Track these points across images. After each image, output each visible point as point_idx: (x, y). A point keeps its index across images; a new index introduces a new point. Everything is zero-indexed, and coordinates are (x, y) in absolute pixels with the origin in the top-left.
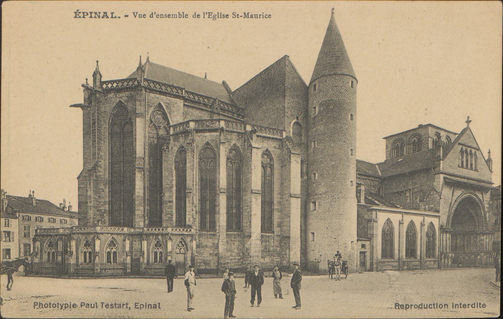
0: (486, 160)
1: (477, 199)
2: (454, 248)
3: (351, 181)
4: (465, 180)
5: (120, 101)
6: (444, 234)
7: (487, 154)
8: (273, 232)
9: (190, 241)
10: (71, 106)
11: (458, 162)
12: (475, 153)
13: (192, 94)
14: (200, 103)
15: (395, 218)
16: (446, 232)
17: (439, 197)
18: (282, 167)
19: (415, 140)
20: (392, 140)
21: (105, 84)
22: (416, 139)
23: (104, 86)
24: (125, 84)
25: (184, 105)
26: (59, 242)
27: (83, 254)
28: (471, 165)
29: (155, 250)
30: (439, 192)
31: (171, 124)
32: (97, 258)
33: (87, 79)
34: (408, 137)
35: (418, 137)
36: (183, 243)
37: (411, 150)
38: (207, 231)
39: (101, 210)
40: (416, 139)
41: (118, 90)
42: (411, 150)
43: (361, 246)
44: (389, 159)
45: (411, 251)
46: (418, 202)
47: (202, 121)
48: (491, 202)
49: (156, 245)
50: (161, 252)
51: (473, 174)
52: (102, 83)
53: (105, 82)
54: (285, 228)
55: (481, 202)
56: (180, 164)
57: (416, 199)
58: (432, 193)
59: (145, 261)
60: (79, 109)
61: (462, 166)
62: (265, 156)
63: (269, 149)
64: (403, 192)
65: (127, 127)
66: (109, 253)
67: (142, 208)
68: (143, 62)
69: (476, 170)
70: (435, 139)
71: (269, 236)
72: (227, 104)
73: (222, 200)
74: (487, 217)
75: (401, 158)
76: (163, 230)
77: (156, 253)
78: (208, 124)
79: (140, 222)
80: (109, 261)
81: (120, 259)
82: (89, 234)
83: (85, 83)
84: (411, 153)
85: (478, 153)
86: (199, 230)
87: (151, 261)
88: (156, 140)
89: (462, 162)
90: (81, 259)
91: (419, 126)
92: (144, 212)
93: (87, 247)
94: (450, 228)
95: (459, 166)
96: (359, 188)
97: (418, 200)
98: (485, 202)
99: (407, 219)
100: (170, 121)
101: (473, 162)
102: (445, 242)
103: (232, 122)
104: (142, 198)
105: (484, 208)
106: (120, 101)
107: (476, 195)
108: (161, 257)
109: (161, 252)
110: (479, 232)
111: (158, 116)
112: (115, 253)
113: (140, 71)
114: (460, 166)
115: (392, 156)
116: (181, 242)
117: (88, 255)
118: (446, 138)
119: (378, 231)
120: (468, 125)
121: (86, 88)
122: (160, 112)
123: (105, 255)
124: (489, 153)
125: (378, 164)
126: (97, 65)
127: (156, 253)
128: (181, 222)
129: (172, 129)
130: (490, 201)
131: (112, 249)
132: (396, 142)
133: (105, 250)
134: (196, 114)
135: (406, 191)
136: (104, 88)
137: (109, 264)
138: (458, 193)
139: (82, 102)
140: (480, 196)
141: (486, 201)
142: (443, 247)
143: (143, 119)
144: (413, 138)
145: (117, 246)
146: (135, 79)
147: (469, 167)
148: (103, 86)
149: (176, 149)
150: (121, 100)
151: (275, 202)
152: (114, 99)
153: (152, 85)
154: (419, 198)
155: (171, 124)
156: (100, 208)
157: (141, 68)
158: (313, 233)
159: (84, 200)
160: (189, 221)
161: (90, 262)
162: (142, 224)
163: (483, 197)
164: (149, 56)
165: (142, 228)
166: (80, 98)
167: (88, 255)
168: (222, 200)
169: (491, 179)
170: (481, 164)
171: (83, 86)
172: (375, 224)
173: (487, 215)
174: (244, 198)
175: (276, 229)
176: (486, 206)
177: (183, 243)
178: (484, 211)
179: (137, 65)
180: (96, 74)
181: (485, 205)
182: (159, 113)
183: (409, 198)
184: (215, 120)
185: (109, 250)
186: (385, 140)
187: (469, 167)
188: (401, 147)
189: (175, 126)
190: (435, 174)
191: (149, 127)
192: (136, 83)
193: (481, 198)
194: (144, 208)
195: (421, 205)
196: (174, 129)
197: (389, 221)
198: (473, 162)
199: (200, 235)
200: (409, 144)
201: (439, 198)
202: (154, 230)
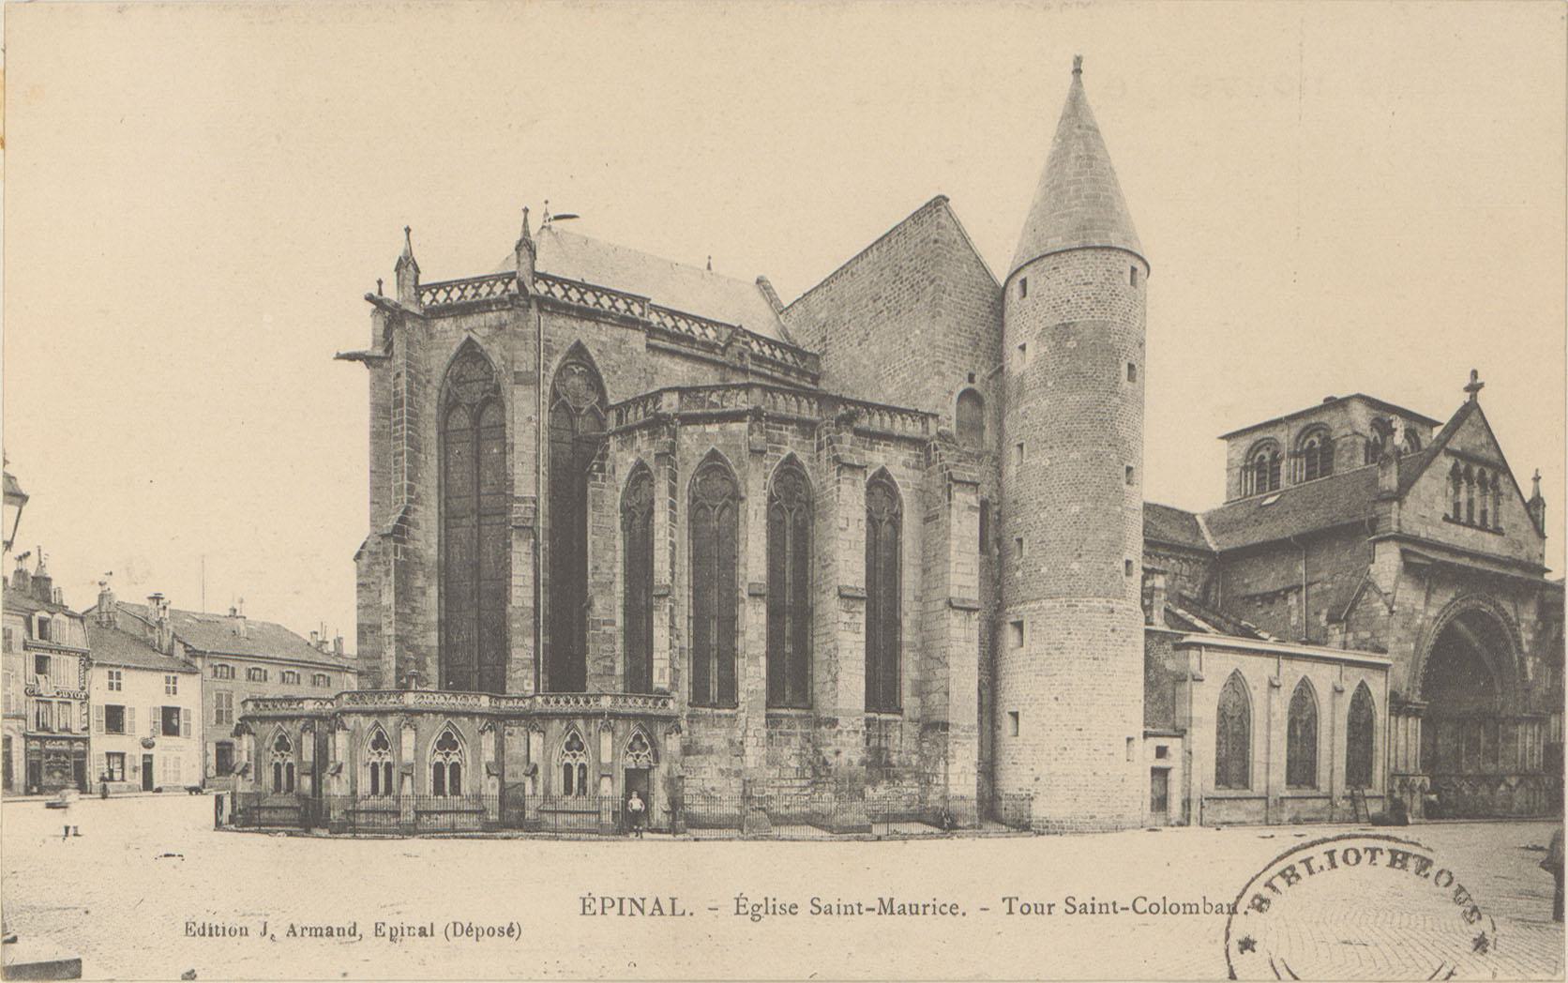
0: (1527, 501)
1: (1501, 618)
2: (1430, 761)
3: (1128, 563)
4: (1465, 561)
5: (469, 339)
6: (1400, 720)
7: (1531, 484)
8: (900, 711)
9: (665, 734)
11: (1444, 507)
12: (1495, 478)
13: (672, 313)
14: (692, 340)
15: (1257, 671)
16: (1408, 714)
17: (1385, 608)
18: (926, 520)
19: (1312, 443)
20: (1245, 443)
21: (427, 293)
22: (1316, 440)
23: (427, 298)
24: (484, 290)
25: (649, 346)
26: (304, 738)
28: (1484, 513)
29: (568, 760)
30: (1386, 594)
31: (612, 402)
32: (408, 780)
33: (380, 282)
34: (1294, 431)
35: (1322, 432)
36: (645, 740)
37: (1301, 470)
38: (714, 706)
39: (418, 647)
40: (1316, 440)
41: (464, 310)
42: (1301, 470)
43: (1154, 752)
44: (1234, 498)
45: (1302, 769)
46: (1324, 624)
47: (697, 389)
48: (1539, 627)
49: (569, 746)
50: (582, 767)
51: (1492, 544)
52: (420, 291)
53: (429, 287)
55: (1508, 620)
56: (635, 516)
57: (1317, 614)
58: (1365, 597)
59: (540, 792)
60: (359, 365)
61: (1456, 520)
63: (890, 470)
64: (1276, 594)
65: (490, 415)
66: (439, 768)
67: (530, 642)
68: (534, 229)
69: (1498, 531)
70: (1372, 440)
71: (887, 723)
72: (769, 342)
73: (753, 620)
74: (1529, 670)
75: (1274, 495)
76: (587, 702)
77: (568, 768)
78: (714, 396)
79: (523, 681)
80: (438, 789)
82: (383, 713)
83: (375, 294)
84: (1301, 481)
85: (1502, 480)
86: (689, 704)
87: (554, 793)
89: (1457, 506)
90: (365, 784)
91: (1325, 400)
92: (536, 649)
93: (380, 750)
94: (1417, 700)
95: (1446, 518)
96: (1149, 583)
97: (1323, 618)
98: (1523, 625)
99: (1293, 673)
100: (609, 393)
101: (1490, 508)
102: (1402, 743)
103: (783, 392)
105: (1519, 643)
106: (469, 339)
107: (1497, 606)
108: (582, 781)
109: (582, 767)
110: (1503, 716)
112: (455, 769)
113: (524, 251)
114: (1451, 516)
115: (1246, 490)
116: (638, 737)
118: (1406, 436)
119: (1203, 706)
120: (1473, 397)
121: (377, 302)
122: (581, 369)
123: (429, 773)
124: (1537, 479)
126: (408, 239)
128: (639, 679)
129: (613, 415)
130: (1536, 623)
131: (447, 754)
132: (1258, 451)
133: (428, 760)
134: (679, 371)
136: (427, 303)
137: (440, 797)
138: (1444, 597)
140: (1508, 607)
141: (1528, 622)
142: (1397, 757)
143: (531, 391)
144: (1307, 437)
145: (460, 747)
146: (512, 276)
147: (1477, 520)
148: (424, 299)
149: (623, 474)
150: (471, 334)
151: (906, 623)
152: (451, 333)
153: (558, 292)
154: (1325, 611)
155: (612, 402)
156: (415, 642)
157: (526, 246)
158: (1015, 715)
160: (662, 676)
161: (388, 790)
162: (529, 688)
163: (1516, 609)
165: (530, 698)
168: (753, 620)
169: (1542, 556)
170: (1511, 514)
171: (370, 298)
173: (1530, 664)
174: (818, 611)
175: (909, 701)
176: (1527, 636)
177: (645, 740)
178: (1520, 651)
179: (518, 237)
180: (406, 264)
181: (1523, 634)
182: (576, 371)
183: (1295, 612)
184: (735, 387)
185: (439, 759)
186: (1225, 442)
187: (1477, 520)
188: (1271, 463)
189: (622, 408)
190: (1375, 542)
191: (550, 411)
192: (513, 287)
193: (1512, 614)
194: (537, 641)
195: (1331, 632)
196: (620, 416)
197: (1236, 679)
198: (1490, 508)
199: (692, 718)
200: (1295, 455)
201: (1385, 612)
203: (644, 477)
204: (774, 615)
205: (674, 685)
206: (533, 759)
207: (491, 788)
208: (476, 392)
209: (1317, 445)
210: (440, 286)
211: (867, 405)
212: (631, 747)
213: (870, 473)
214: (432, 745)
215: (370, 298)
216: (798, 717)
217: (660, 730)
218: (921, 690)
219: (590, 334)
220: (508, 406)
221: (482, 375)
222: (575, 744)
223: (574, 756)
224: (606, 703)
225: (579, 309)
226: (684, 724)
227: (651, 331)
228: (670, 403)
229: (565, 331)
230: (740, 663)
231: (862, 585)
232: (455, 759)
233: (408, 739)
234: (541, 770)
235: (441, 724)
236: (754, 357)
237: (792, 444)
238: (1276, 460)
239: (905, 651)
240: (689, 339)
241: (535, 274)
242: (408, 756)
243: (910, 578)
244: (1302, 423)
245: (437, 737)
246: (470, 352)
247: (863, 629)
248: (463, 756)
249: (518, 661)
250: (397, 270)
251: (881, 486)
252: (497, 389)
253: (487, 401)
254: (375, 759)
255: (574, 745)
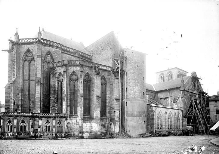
10: (3, 50)
13: (66, 47)
18: (111, 85)
20: (159, 74)
27: (7, 127)
29: (47, 125)
33: (11, 38)
49: (47, 122)
50: (49, 126)
54: (112, 115)
60: (7, 52)
62: (103, 79)
65: (32, 63)
67: (39, 104)
73: (81, 101)
77: (47, 126)
79: (37, 111)
81: (27, 129)
82: (12, 116)
88: (47, 69)
97: (172, 102)
104: (40, 98)
109: (49, 126)
111: (48, 57)
112: (25, 127)
113: (40, 34)
116: (60, 121)
117: (10, 127)
121: (11, 42)
125: (153, 85)
127: (47, 126)
129: (55, 64)
131: (23, 124)
134: (67, 57)
135: (167, 98)
139: (8, 49)
146: (37, 38)
148: (20, 41)
151: (107, 102)
152: (25, 48)
154: (173, 101)
155: (55, 62)
157: (40, 33)
159: (8, 99)
160: (64, 110)
162: (39, 112)
164: (44, 27)
166: (8, 46)
167: (10, 127)
171: (9, 40)
172: (154, 113)
175: (108, 115)
179: (38, 32)
180: (17, 34)
185: (22, 125)
186: (156, 74)
194: (41, 104)
196: (57, 64)
202: (47, 114)
203: (61, 75)
204: (85, 99)
205: (67, 112)
206: (40, 125)
207: (31, 130)
208: (29, 58)
209: (170, 75)
210: (23, 39)
211: (101, 65)
212: (58, 123)
213: (101, 76)
214: (20, 122)
215: (9, 40)
216: (89, 117)
217: (64, 119)
218: (110, 113)
219: (52, 50)
220: (36, 61)
221: (31, 56)
222: (48, 122)
223: (48, 124)
224: (54, 115)
225: (49, 45)
226: (68, 118)
227: (62, 50)
228: (66, 62)
229: (48, 48)
230: (78, 108)
231: (100, 95)
232: (25, 125)
233: (15, 121)
234: (41, 127)
235: (22, 118)
236: (80, 55)
237: (87, 70)
238: (164, 77)
239: (107, 106)
240: (69, 52)
241: (41, 38)
242: (15, 124)
243: (108, 93)
244: (168, 71)
245: (21, 121)
246: (28, 51)
247: (100, 102)
248: (26, 124)
249: (37, 107)
250: (15, 36)
251: (103, 78)
252: (34, 58)
253: (32, 60)
254: (9, 125)
255: (48, 122)
